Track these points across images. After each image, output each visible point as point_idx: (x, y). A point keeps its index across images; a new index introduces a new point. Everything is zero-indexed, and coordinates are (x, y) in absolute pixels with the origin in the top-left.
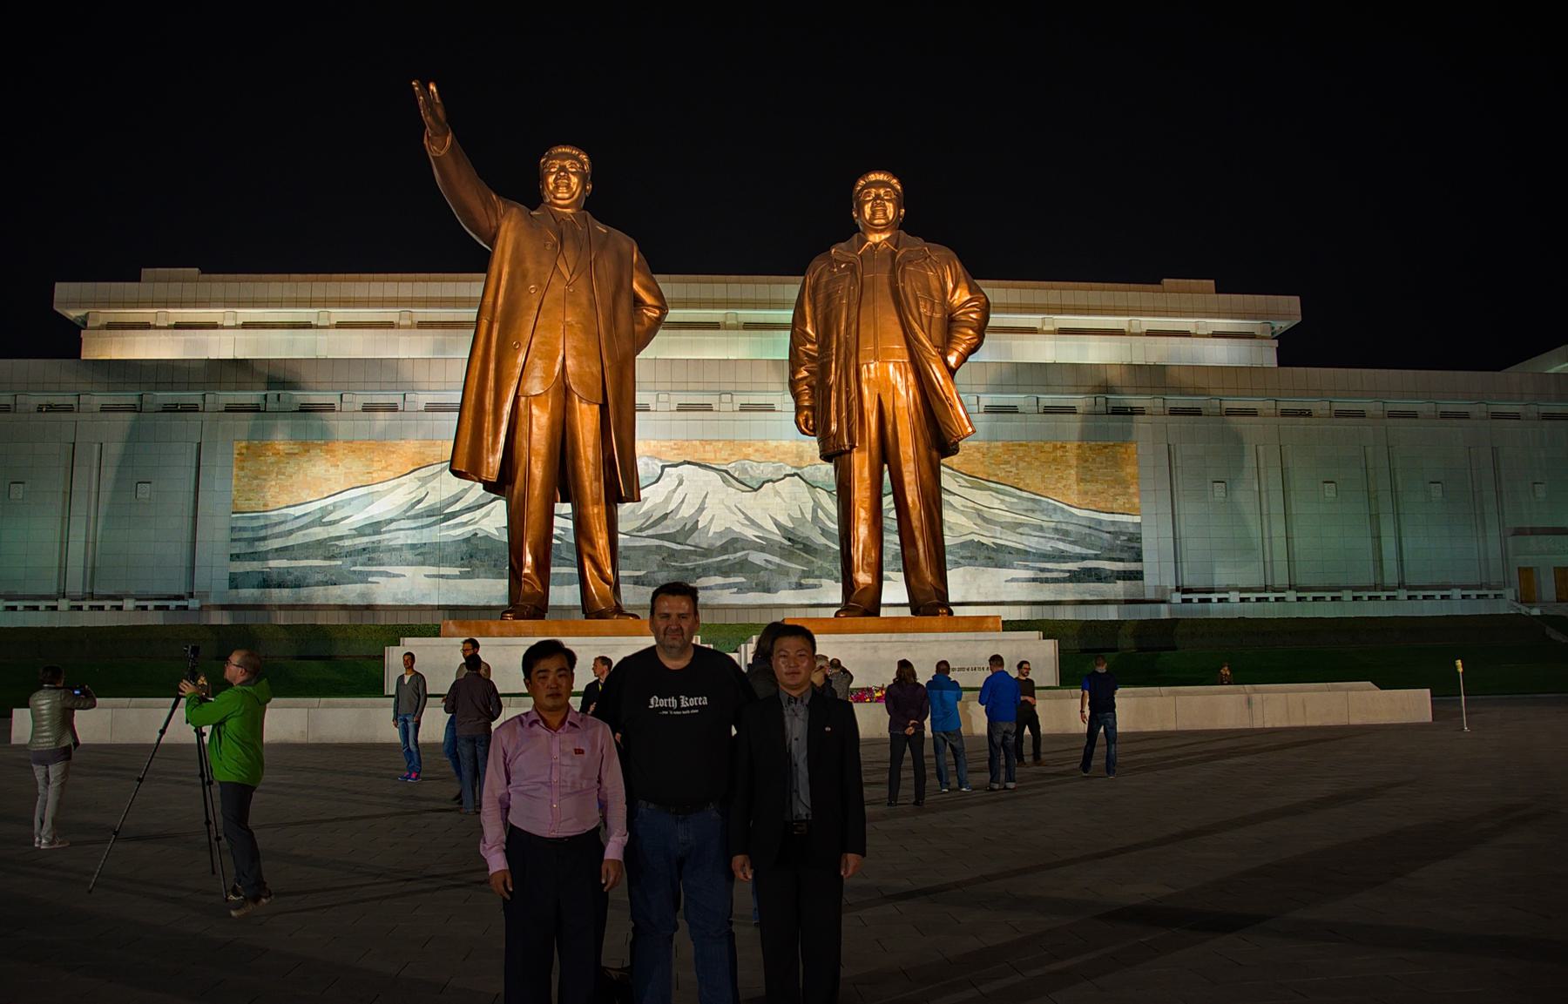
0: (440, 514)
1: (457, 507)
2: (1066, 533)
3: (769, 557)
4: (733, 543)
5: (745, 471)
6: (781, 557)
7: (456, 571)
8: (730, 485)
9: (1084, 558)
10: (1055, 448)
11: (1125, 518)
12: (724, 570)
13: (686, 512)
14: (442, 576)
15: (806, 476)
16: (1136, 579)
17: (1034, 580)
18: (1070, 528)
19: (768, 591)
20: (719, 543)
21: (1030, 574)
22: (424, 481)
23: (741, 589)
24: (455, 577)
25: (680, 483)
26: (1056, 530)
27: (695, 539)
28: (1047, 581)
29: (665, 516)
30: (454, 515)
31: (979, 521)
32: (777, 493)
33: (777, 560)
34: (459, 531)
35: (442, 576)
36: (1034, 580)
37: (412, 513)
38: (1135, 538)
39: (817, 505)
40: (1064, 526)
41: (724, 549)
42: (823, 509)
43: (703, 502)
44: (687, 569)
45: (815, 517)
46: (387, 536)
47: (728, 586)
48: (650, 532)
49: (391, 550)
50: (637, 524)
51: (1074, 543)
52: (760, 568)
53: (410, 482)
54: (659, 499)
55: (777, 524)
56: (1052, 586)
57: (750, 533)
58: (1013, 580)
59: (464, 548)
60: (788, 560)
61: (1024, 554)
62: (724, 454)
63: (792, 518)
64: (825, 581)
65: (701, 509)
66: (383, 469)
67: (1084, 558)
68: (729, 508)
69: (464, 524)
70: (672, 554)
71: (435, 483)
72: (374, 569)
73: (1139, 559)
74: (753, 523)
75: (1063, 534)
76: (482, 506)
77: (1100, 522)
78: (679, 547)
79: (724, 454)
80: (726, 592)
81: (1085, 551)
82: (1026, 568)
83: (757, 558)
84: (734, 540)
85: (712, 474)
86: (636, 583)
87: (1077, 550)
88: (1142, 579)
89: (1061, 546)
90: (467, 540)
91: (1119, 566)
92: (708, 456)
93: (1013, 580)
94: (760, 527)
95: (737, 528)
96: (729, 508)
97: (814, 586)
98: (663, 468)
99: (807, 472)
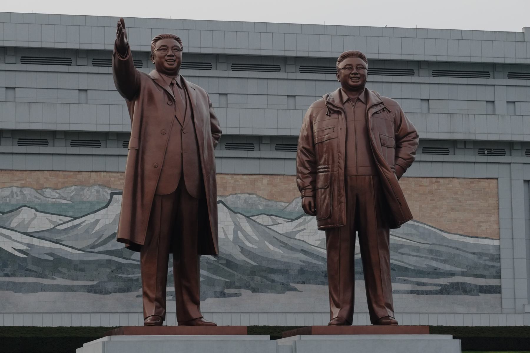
11: (486, 242)
15: (229, 204)
16: (495, 292)
17: (412, 292)
26: (431, 251)
28: (422, 293)
36: (412, 292)
38: (498, 259)
40: (437, 248)
42: (243, 231)
44: (131, 280)
48: (101, 249)
50: (91, 242)
51: (445, 261)
56: (426, 297)
60: (215, 273)
64: (244, 292)
67: (452, 274)
70: (120, 267)
73: (498, 276)
75: (434, 254)
77: (465, 244)
81: (453, 269)
82: (406, 282)
86: (89, 291)
87: (447, 267)
88: (500, 292)
89: (434, 264)
91: (482, 282)
97: (236, 295)
98: (112, 194)
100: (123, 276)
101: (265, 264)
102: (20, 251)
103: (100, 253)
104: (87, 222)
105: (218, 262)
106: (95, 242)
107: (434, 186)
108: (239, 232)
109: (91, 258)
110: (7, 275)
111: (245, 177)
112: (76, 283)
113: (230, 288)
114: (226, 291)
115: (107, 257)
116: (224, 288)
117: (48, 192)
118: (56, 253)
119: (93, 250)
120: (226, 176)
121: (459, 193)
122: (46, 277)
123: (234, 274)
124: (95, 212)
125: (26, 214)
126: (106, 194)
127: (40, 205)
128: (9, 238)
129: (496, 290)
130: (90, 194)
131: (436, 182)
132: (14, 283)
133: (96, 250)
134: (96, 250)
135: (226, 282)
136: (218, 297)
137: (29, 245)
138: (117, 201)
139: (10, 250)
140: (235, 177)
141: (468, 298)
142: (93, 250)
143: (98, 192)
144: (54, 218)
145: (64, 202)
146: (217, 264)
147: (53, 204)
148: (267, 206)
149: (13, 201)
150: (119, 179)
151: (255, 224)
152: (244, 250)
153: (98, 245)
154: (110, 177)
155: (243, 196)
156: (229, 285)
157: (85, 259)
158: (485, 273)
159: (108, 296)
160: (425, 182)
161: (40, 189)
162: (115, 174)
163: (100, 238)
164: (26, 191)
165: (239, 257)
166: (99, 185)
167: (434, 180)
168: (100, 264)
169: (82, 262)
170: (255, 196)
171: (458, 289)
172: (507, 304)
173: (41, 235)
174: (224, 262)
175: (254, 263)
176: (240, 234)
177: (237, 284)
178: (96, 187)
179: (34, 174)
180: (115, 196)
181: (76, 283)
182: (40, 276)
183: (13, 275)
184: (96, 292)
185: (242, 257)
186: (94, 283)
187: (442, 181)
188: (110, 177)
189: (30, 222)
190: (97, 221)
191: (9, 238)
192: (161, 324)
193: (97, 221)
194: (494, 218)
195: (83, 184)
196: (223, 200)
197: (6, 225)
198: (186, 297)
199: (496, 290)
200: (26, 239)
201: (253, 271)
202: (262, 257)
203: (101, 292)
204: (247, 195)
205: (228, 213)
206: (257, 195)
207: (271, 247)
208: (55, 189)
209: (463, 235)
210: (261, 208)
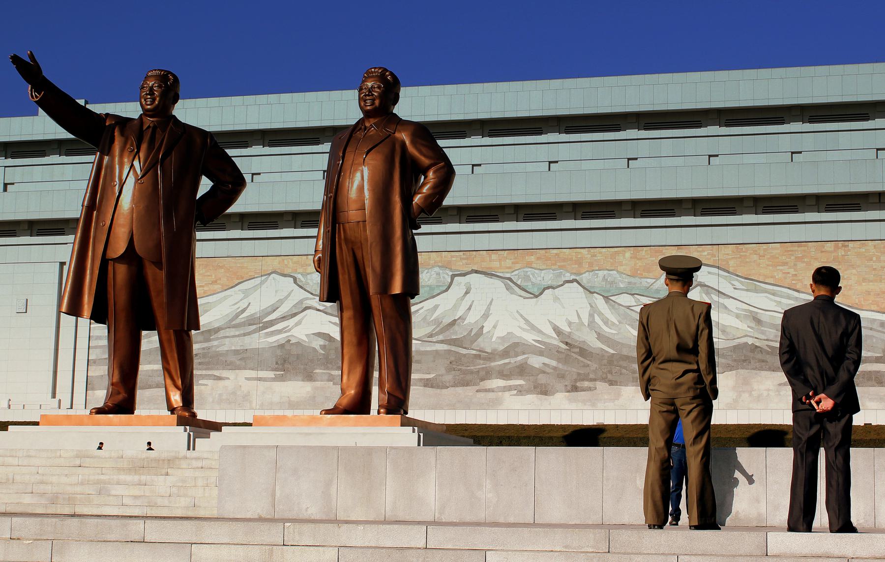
0: (260, 323)
3: (547, 361)
4: (514, 348)
5: (527, 278)
6: (559, 360)
7: (271, 374)
8: (513, 293)
10: (837, 248)
12: (503, 374)
13: (472, 318)
14: (260, 379)
15: (584, 282)
20: (501, 348)
22: (247, 293)
23: (521, 391)
27: (481, 343)
29: (453, 323)
30: (272, 323)
31: (753, 325)
32: (556, 299)
33: (554, 363)
35: (260, 379)
37: (237, 321)
41: (505, 354)
42: (600, 314)
43: (488, 308)
44: (472, 372)
45: (592, 324)
46: (215, 343)
47: (509, 388)
48: (441, 337)
49: (218, 355)
50: (429, 330)
53: (235, 294)
55: (557, 330)
57: (530, 337)
59: (279, 352)
62: (509, 263)
63: (570, 324)
64: (601, 386)
65: (486, 316)
66: (215, 282)
69: (279, 332)
70: (459, 358)
72: (204, 372)
74: (533, 328)
76: (295, 315)
80: (507, 394)
83: (536, 361)
84: (516, 345)
86: (425, 386)
90: (282, 346)
94: (540, 332)
95: (519, 333)
97: (589, 389)
99: (585, 278)
100: (463, 368)
101: (625, 352)
103: (442, 342)
104: (425, 309)
105: (569, 350)
106: (434, 330)
107: (841, 252)
108: (596, 315)
109: (428, 349)
111: (604, 250)
113: (583, 380)
114: (578, 384)
115: (445, 347)
116: (576, 381)
119: (430, 339)
120: (582, 250)
121: (874, 259)
123: (588, 366)
124: (433, 297)
126: (446, 276)
131: (843, 246)
133: (434, 339)
134: (434, 339)
135: (579, 374)
136: (569, 392)
138: (459, 284)
140: (592, 250)
142: (430, 339)
143: (438, 274)
146: (569, 353)
148: (630, 283)
150: (461, 259)
152: (600, 337)
153: (437, 334)
154: (452, 257)
155: (601, 273)
156: (585, 378)
157: (422, 349)
159: (444, 391)
160: (829, 247)
162: (457, 254)
163: (438, 326)
165: (594, 343)
166: (439, 267)
167: (840, 244)
170: (615, 272)
171: (870, 379)
174: (578, 350)
175: (612, 352)
176: (597, 319)
177: (592, 376)
178: (437, 269)
180: (456, 278)
184: (432, 387)
185: (599, 345)
187: (851, 244)
188: (452, 257)
190: (436, 307)
192: (133, 413)
193: (436, 307)
196: (577, 278)
198: (169, 381)
202: (622, 344)
203: (438, 387)
204: (606, 272)
205: (584, 296)
206: (618, 271)
209: (879, 312)
210: (622, 286)
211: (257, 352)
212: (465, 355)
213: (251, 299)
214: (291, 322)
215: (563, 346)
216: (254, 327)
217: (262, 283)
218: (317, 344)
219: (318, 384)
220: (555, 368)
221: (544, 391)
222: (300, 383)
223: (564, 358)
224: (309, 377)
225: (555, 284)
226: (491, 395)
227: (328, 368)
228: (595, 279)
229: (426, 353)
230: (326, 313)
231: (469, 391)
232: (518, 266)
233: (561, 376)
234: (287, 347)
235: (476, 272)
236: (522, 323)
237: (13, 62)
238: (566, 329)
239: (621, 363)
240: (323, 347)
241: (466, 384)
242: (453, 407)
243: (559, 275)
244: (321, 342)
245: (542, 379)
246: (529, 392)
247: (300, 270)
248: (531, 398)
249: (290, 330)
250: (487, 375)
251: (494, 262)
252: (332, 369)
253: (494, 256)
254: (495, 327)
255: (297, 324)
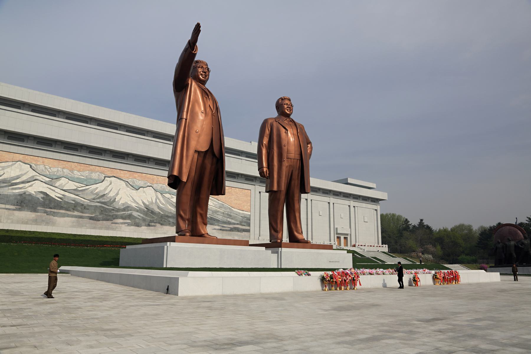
1: (18, 181)
2: (230, 216)
3: (139, 214)
4: (127, 208)
5: (134, 183)
6: (144, 214)
9: (234, 224)
11: (246, 213)
13: (112, 195)
14: (7, 209)
17: (221, 230)
18: (232, 214)
19: (138, 226)
20: (122, 207)
21: (219, 228)
22: (3, 168)
23: (129, 225)
24: (14, 210)
25: (111, 184)
26: (228, 214)
28: (223, 230)
30: (16, 184)
32: (144, 192)
33: (142, 215)
34: (17, 191)
35: (7, 209)
36: (221, 230)
38: (250, 220)
39: (157, 198)
40: (229, 213)
41: (124, 210)
42: (159, 199)
44: (110, 216)
45: (156, 201)
47: (125, 223)
48: (98, 200)
50: (93, 197)
52: (136, 218)
54: (102, 189)
57: (134, 205)
58: (215, 229)
61: (218, 221)
62: (128, 175)
65: (117, 194)
67: (234, 224)
68: (127, 195)
70: (106, 210)
71: (8, 170)
73: (249, 225)
74: (135, 201)
77: (239, 213)
78: (108, 207)
79: (128, 175)
80: (123, 225)
82: (219, 225)
83: (135, 214)
84: (128, 207)
85: (122, 182)
87: (233, 221)
89: (229, 220)
91: (244, 227)
92: (121, 174)
93: (215, 229)
94: (138, 203)
96: (127, 195)
97: (154, 226)
98: (105, 177)
99: (155, 186)
101: (167, 214)
102: (58, 197)
107: (230, 190)
110: (51, 208)
112: (84, 215)
116: (150, 222)
117: (75, 172)
118: (76, 200)
122: (70, 211)
125: (63, 181)
127: (71, 177)
128: (54, 191)
129: (248, 231)
130: (95, 176)
132: (54, 212)
137: (63, 195)
139: (54, 197)
141: (239, 233)
144: (77, 184)
145: (83, 177)
147: (77, 178)
149: (58, 174)
151: (164, 197)
152: (159, 207)
153: (97, 199)
157: (90, 204)
158: (245, 224)
161: (72, 170)
164: (65, 170)
165: (157, 210)
168: (96, 206)
169: (88, 205)
172: (252, 236)
173: (70, 191)
178: (98, 173)
179: (70, 163)
181: (84, 215)
182: (67, 209)
183: (54, 209)
186: (93, 215)
189: (65, 185)
190: (97, 188)
191: (54, 191)
193: (97, 188)
194: (249, 204)
195: (92, 171)
197: (53, 184)
199: (248, 231)
200: (63, 192)
201: (162, 217)
203: (95, 220)
207: (170, 207)
208: (79, 171)
211: (7, 196)
212: (107, 209)
213: (5, 171)
214: (27, 185)
215: (146, 209)
216: (6, 184)
217: (12, 165)
218: (40, 196)
219: (39, 214)
220: (143, 217)
221: (138, 225)
222: (29, 213)
223: (146, 213)
224: (35, 210)
225: (144, 186)
226: (117, 225)
227: (44, 207)
228: (158, 187)
229: (91, 206)
230: (46, 183)
231: (109, 223)
232: (131, 177)
233: (144, 220)
234: (24, 196)
235: (114, 177)
236: (131, 199)
237: (196, 26)
238: (147, 203)
239: (166, 218)
240: (43, 198)
241: (108, 220)
242: (101, 228)
243: (146, 183)
244: (42, 196)
245: (137, 221)
246: (132, 225)
247: (34, 163)
248: (132, 227)
249: (26, 188)
250: (117, 217)
251: (121, 174)
252: (47, 208)
253: (122, 172)
254: (120, 199)
255: (30, 186)
